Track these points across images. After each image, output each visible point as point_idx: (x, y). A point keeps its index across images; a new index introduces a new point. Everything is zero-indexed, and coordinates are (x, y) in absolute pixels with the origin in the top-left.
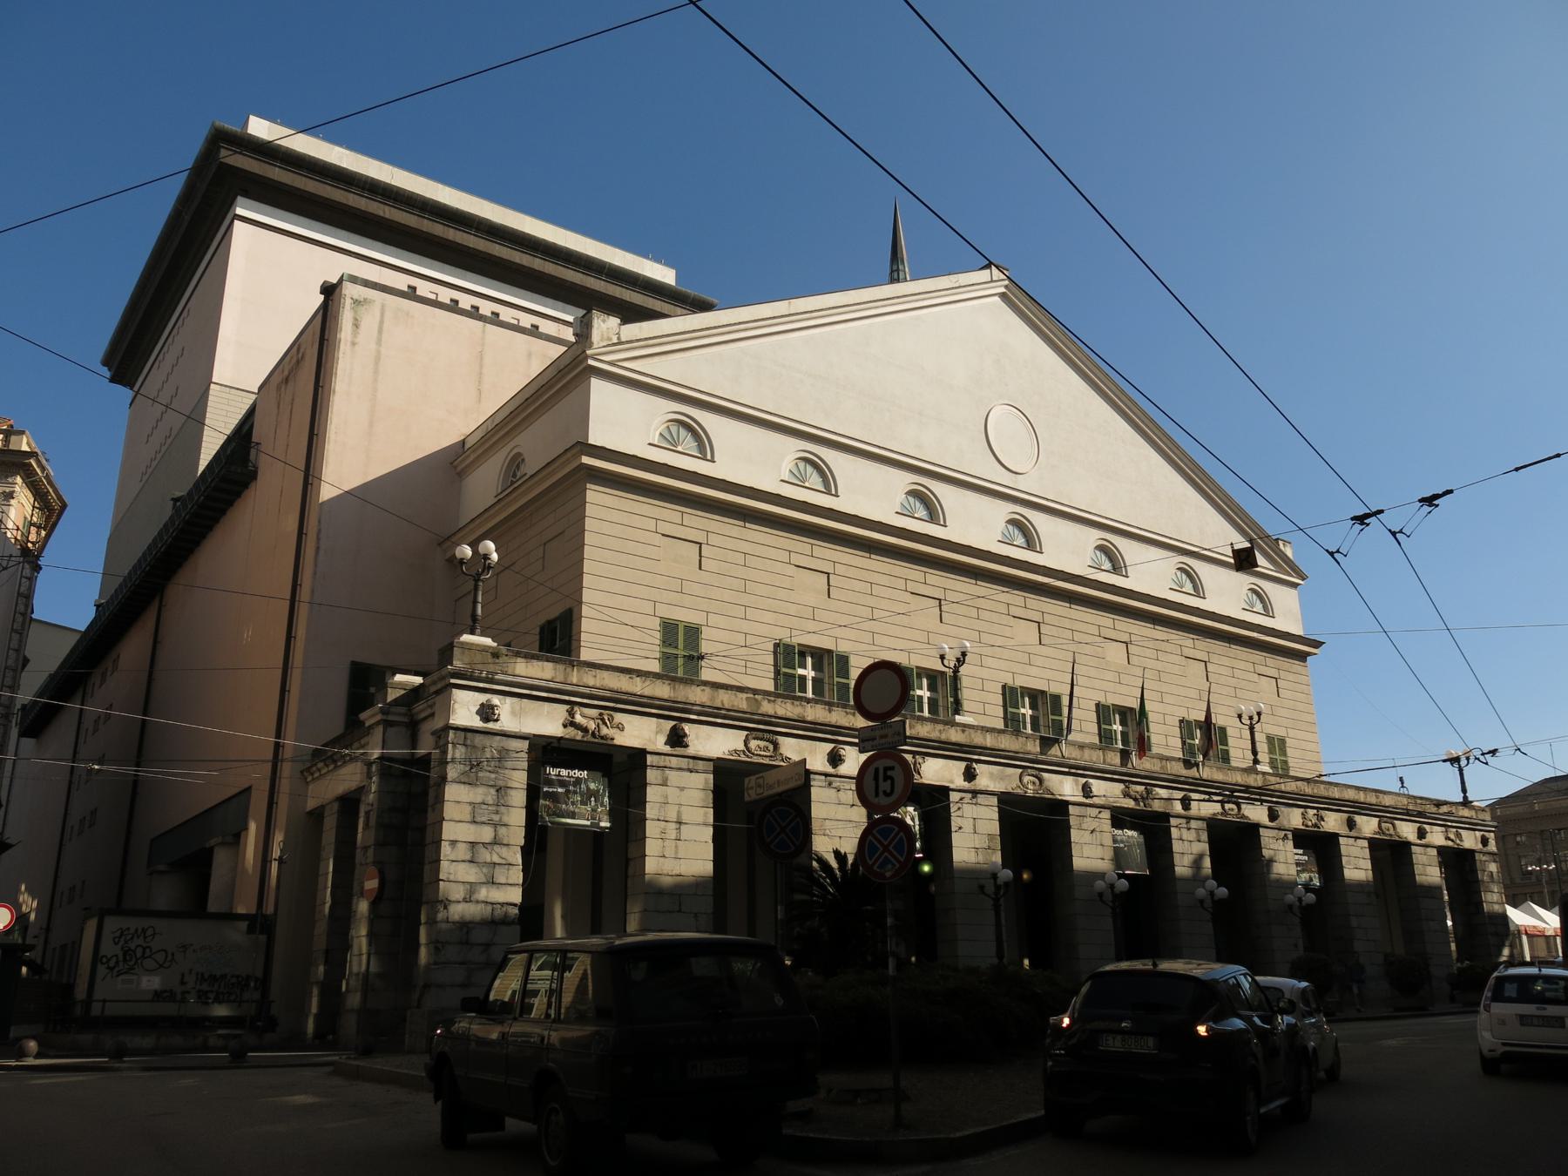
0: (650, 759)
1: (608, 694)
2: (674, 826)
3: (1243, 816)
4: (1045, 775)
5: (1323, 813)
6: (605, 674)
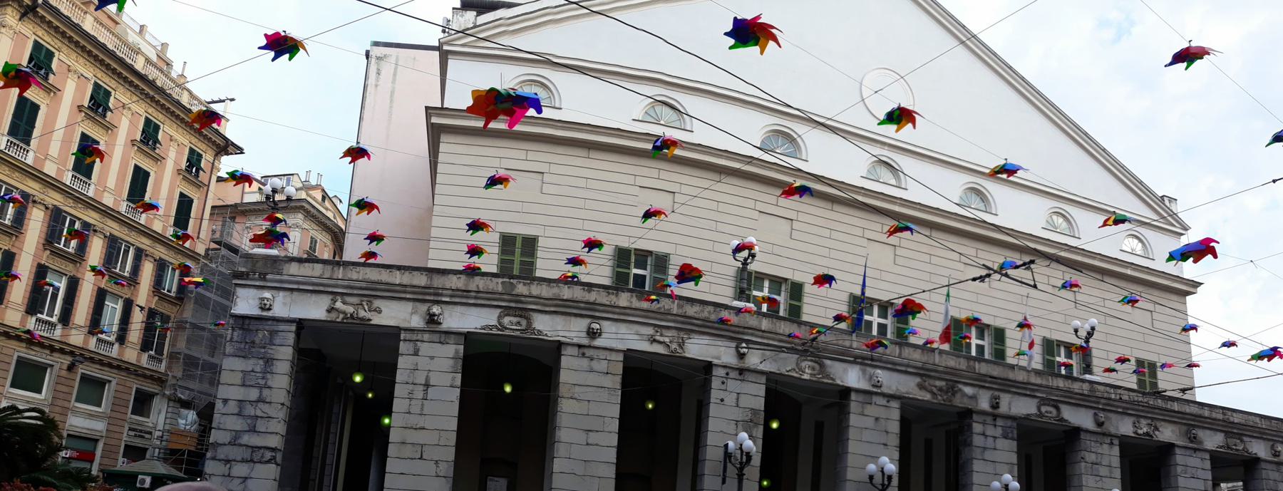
0: (402, 336)
1: (364, 285)
2: (422, 388)
3: (1062, 420)
4: (828, 362)
5: (1158, 424)
6: (368, 270)
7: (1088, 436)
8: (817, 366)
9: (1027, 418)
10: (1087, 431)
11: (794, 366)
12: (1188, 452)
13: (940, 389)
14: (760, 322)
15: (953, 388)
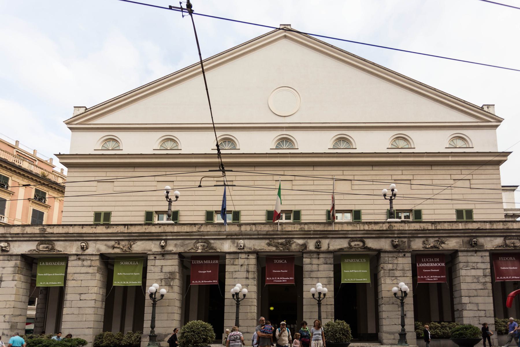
4: (212, 241)
7: (386, 255)
8: (206, 244)
9: (341, 250)
10: (386, 252)
11: (192, 246)
12: (469, 254)
13: (282, 244)
15: (289, 242)
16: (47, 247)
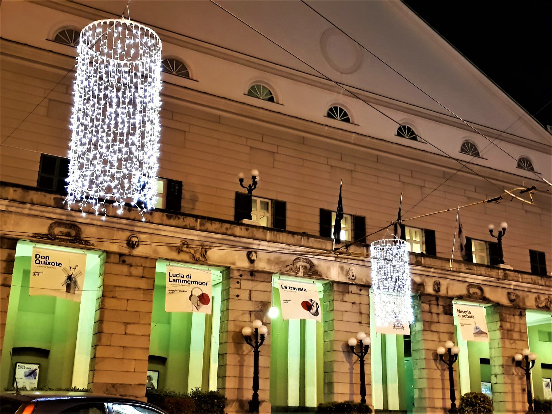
14: (265, 235)
16: (68, 234)
